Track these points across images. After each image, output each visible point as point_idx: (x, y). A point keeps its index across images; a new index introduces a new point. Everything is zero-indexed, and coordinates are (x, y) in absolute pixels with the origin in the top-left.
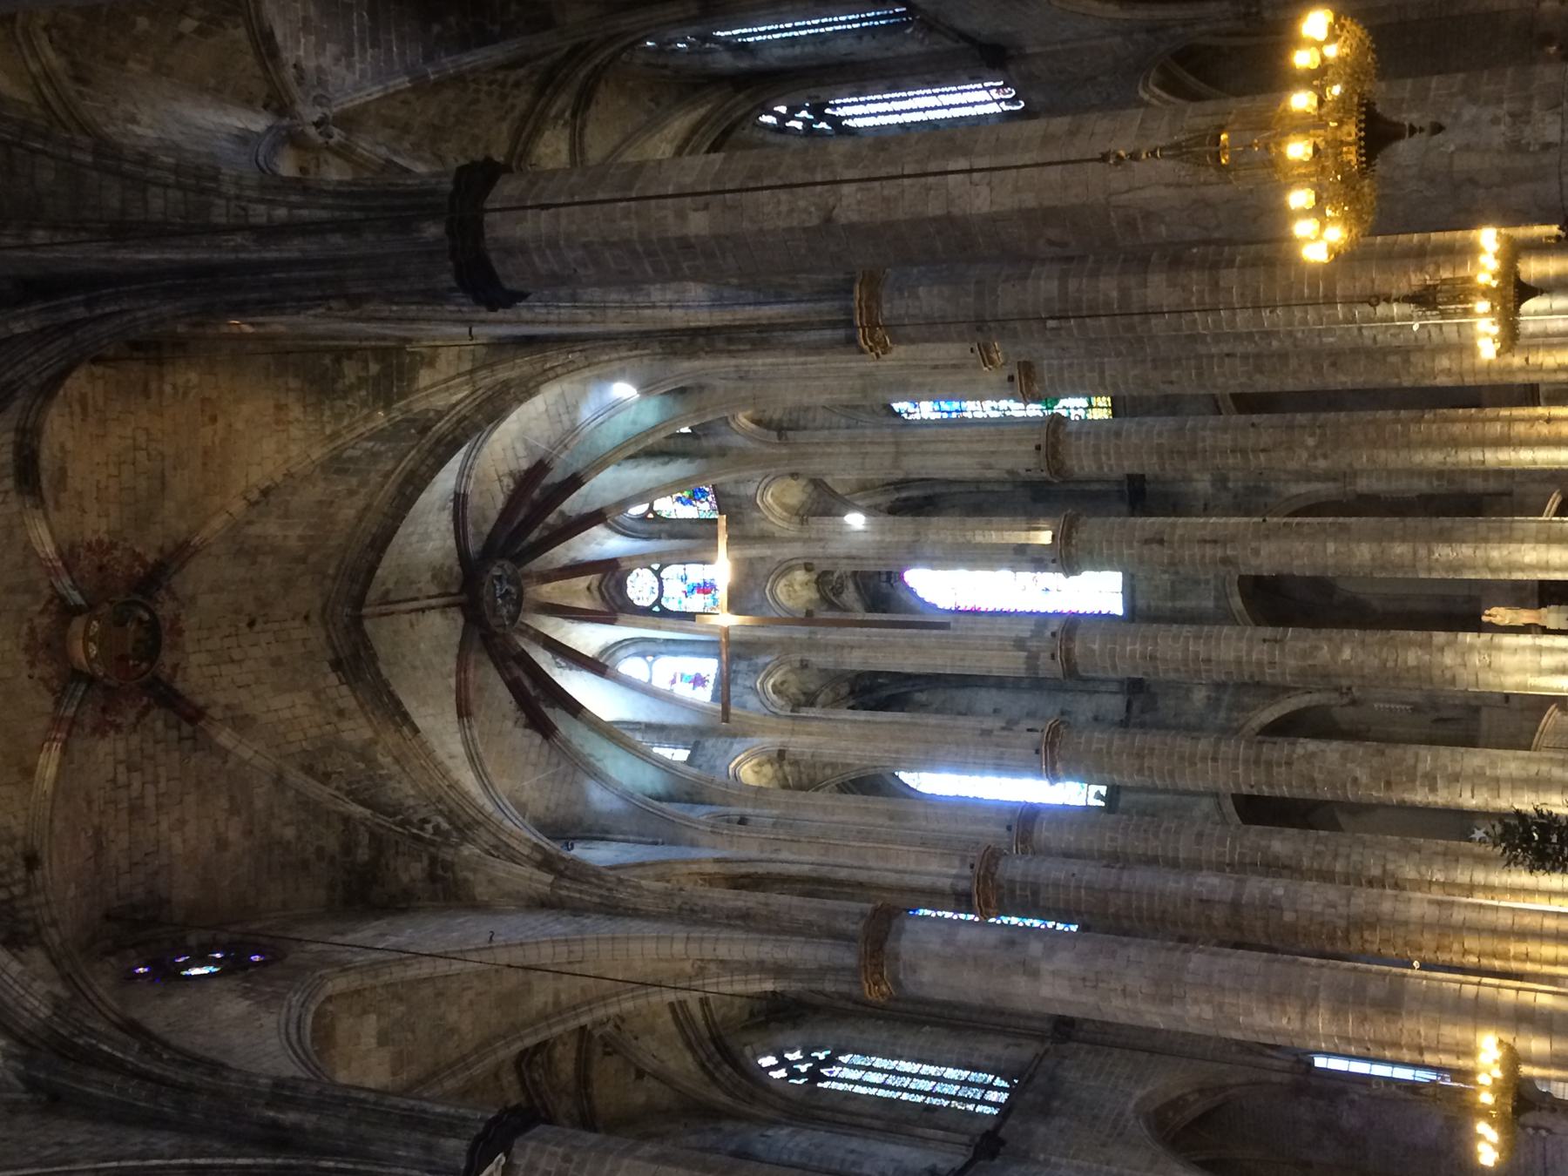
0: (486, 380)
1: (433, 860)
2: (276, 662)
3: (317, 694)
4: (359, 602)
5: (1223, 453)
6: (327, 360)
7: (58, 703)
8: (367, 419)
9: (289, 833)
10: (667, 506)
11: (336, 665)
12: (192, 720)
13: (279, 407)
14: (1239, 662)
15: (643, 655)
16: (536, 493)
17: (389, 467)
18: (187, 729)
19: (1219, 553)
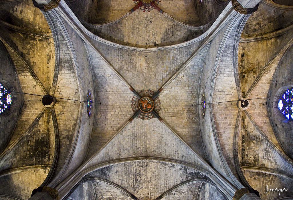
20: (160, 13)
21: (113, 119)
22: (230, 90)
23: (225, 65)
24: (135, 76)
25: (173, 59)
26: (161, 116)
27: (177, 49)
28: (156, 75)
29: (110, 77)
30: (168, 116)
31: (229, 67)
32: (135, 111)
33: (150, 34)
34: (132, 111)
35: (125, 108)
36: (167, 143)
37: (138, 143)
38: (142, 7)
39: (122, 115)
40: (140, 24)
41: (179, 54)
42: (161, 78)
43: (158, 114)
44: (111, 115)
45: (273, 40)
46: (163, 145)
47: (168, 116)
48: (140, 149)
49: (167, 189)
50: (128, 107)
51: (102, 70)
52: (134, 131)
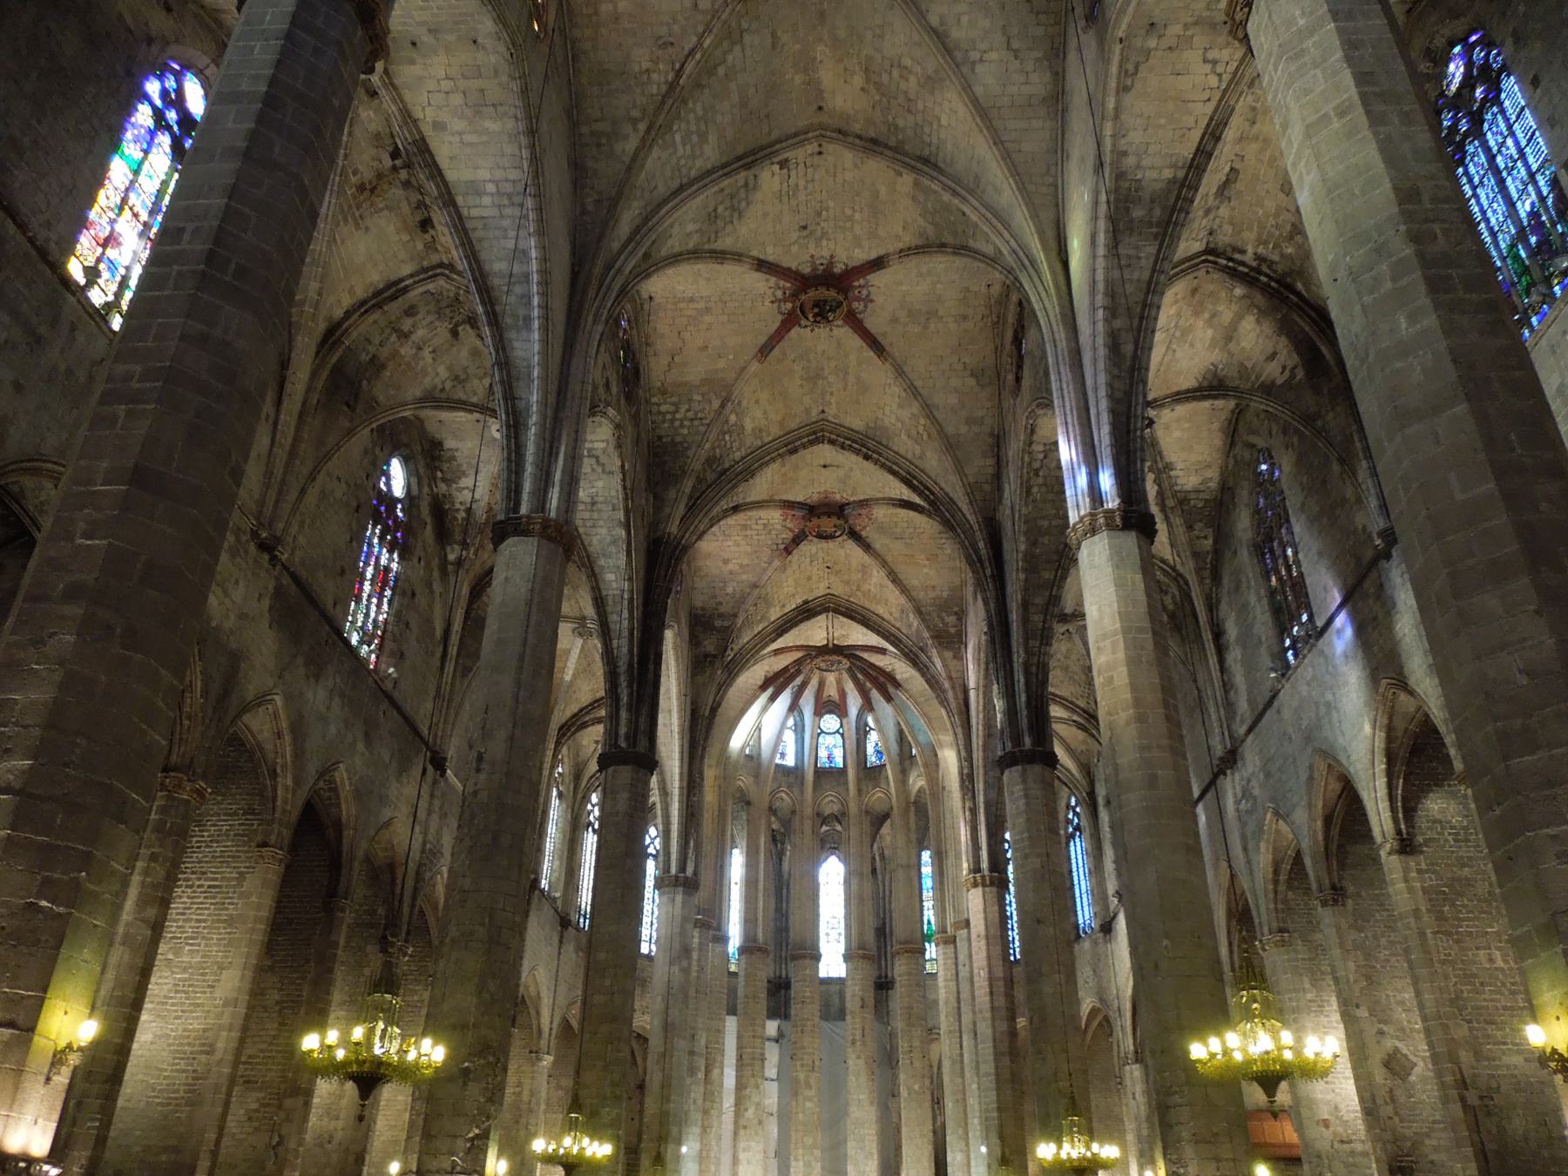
0: (947, 685)
1: (715, 656)
2: (809, 578)
3: (793, 595)
4: (837, 611)
5: (910, 1041)
6: (956, 609)
7: (799, 503)
8: (928, 628)
9: (729, 590)
10: (873, 737)
11: (806, 602)
12: (786, 549)
13: (933, 587)
14: (804, 1048)
15: (795, 725)
16: (882, 679)
17: (904, 631)
18: (782, 547)
19: (858, 1037)
20: (771, 258)
22: (444, 117)
23: (505, 237)
24: (869, 35)
25: (703, 137)
27: (691, 183)
28: (774, 46)
29: (984, 46)
31: (485, 227)
33: (806, 188)
38: (838, 269)
40: (850, 218)
41: (683, 162)
42: (747, 39)
45: (339, 313)
51: (1013, 89)
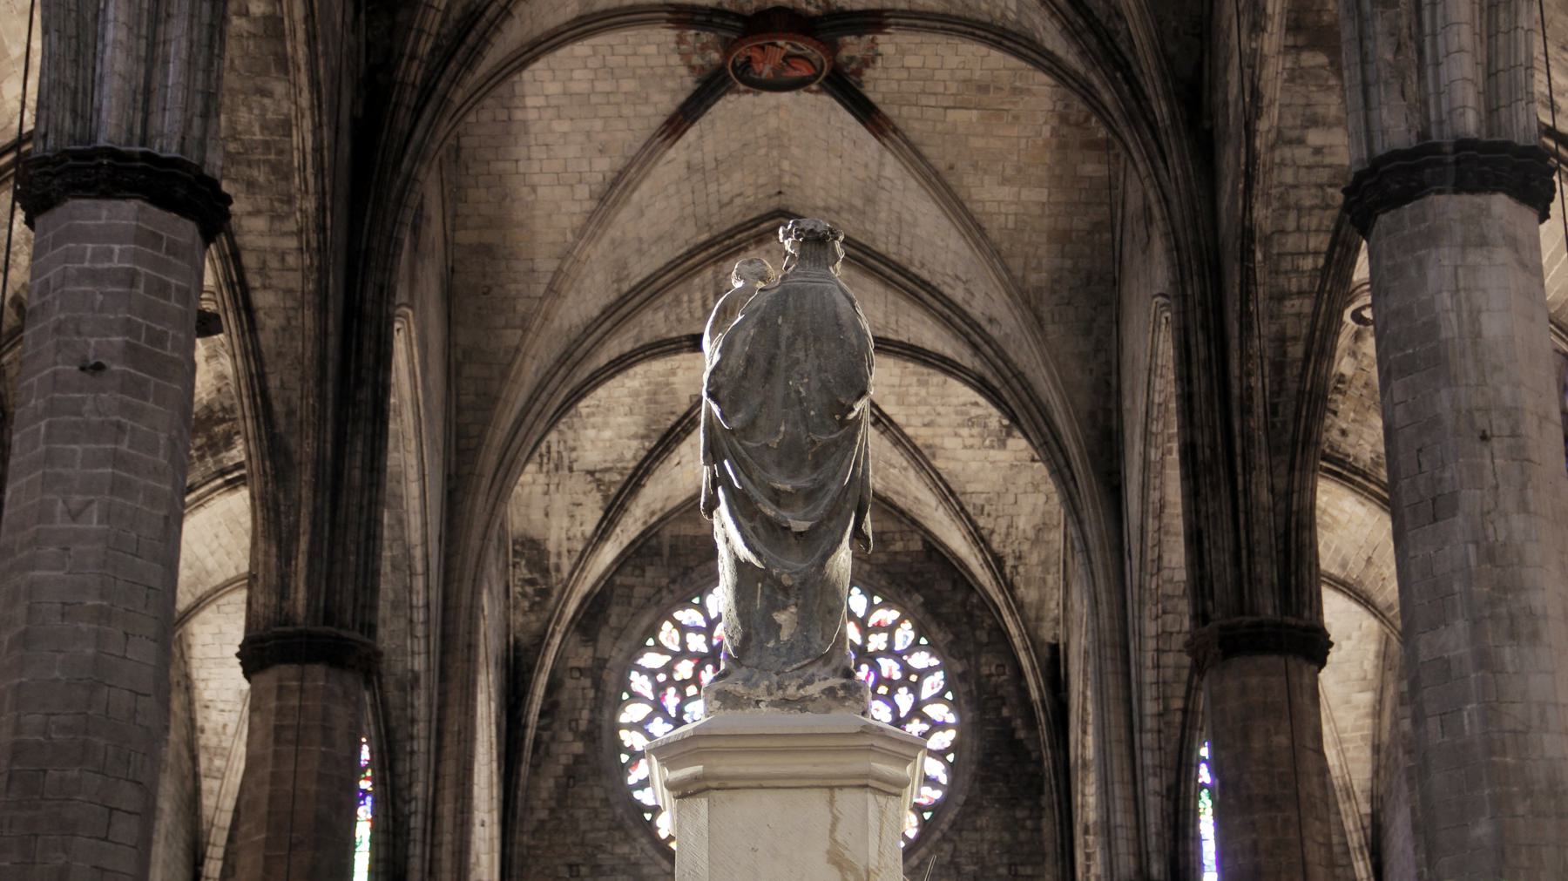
21: (564, 126)
26: (875, 97)
30: (924, 100)
32: (702, 67)
34: (683, 71)
35: (635, 54)
36: (907, 217)
37: (726, 187)
39: (620, 98)
43: (860, 84)
44: (541, 101)
46: (883, 215)
47: (924, 100)
48: (738, 201)
49: (904, 338)
50: (652, 49)
52: (698, 155)
